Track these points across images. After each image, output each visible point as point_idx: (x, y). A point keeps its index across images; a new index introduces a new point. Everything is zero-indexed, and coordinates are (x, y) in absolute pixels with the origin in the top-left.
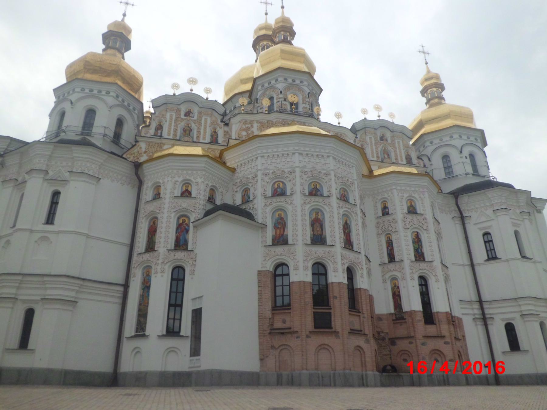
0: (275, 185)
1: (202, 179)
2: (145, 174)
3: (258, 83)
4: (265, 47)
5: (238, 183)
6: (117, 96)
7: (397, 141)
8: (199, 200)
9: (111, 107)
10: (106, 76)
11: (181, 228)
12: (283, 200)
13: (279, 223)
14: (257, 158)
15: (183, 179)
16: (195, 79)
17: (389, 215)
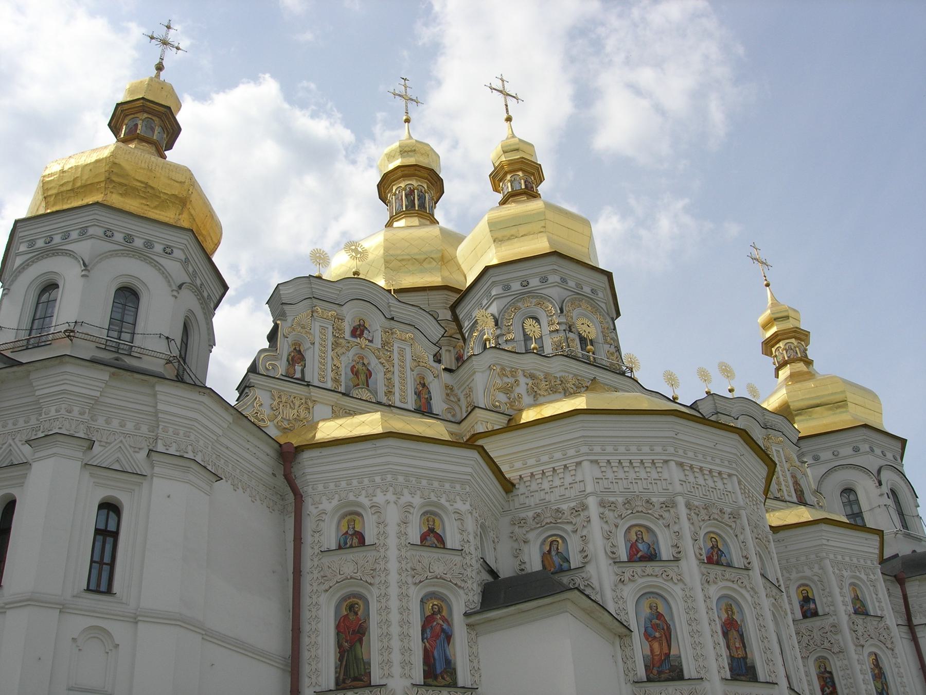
0: (630, 532)
1: (468, 503)
2: (308, 477)
3: (493, 279)
4: (416, 191)
5: (530, 521)
6: (187, 261)
7: (776, 450)
8: (468, 558)
9: (180, 287)
10: (155, 208)
11: (431, 627)
12: (658, 570)
13: (655, 627)
14: (579, 464)
15: (423, 501)
17: (818, 618)
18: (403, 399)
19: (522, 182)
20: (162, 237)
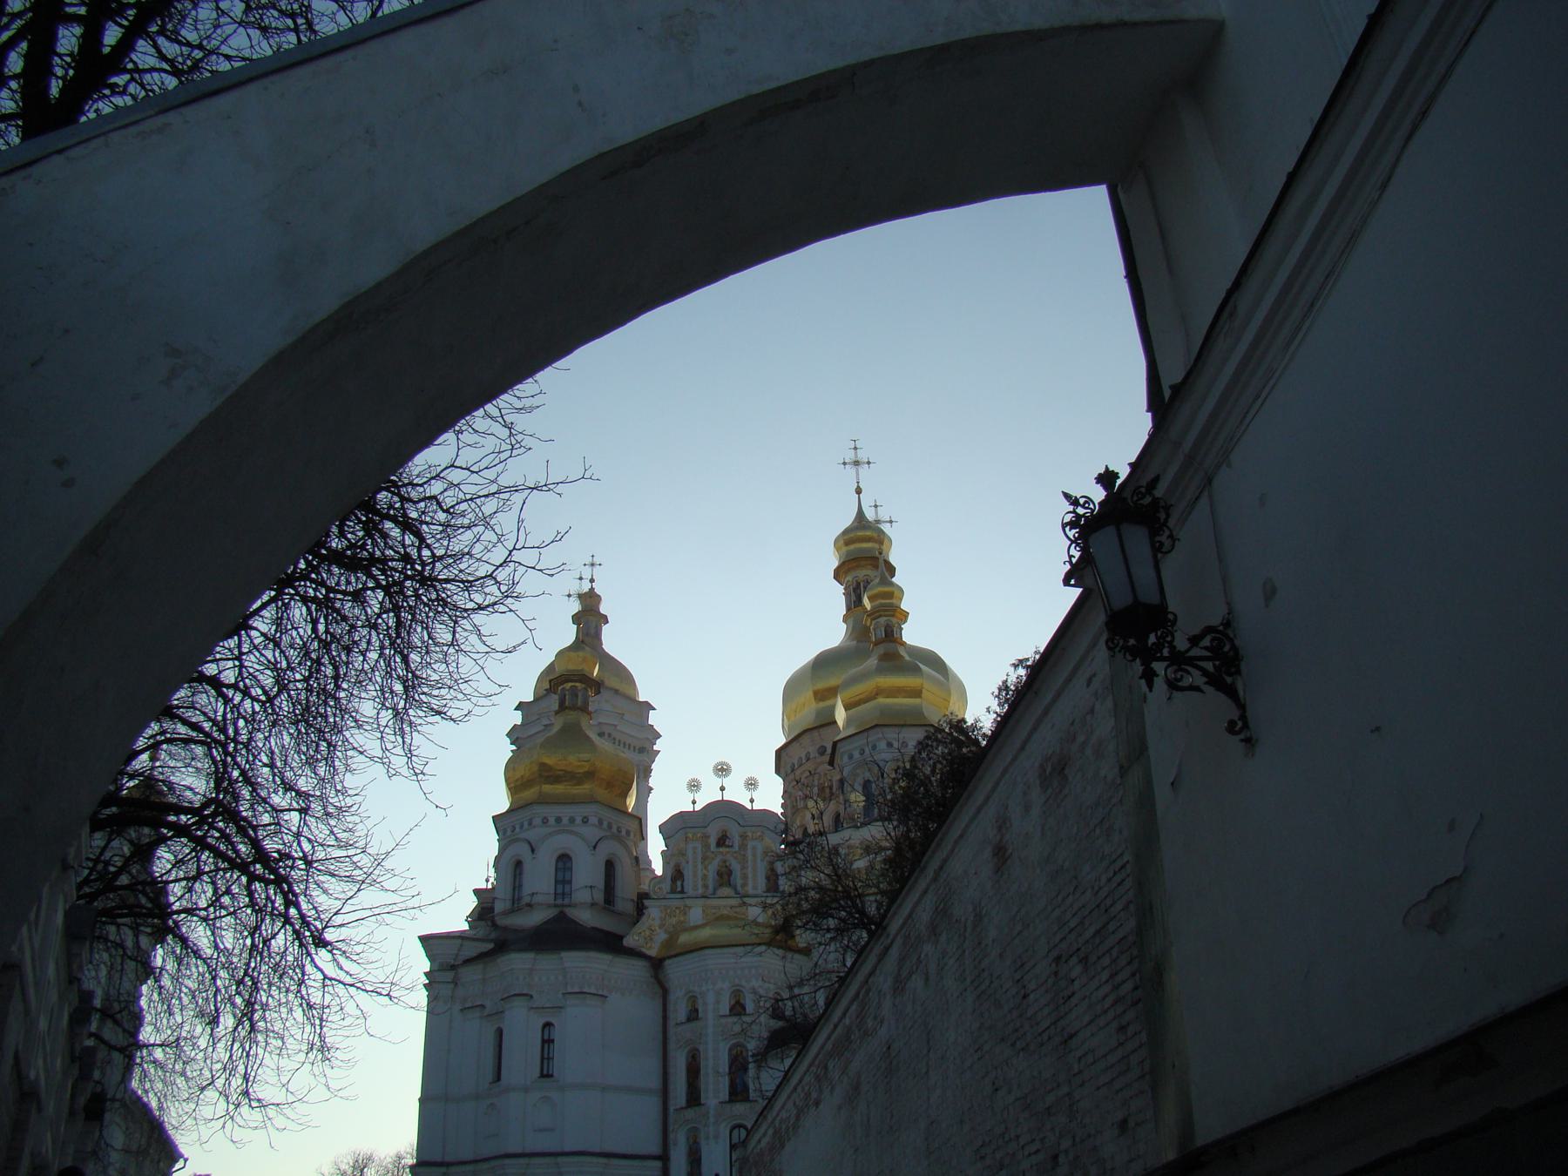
3: (842, 750)
6: (601, 822)
10: (575, 785)
16: (727, 765)
18: (755, 888)
19: (883, 629)
20: (578, 811)
